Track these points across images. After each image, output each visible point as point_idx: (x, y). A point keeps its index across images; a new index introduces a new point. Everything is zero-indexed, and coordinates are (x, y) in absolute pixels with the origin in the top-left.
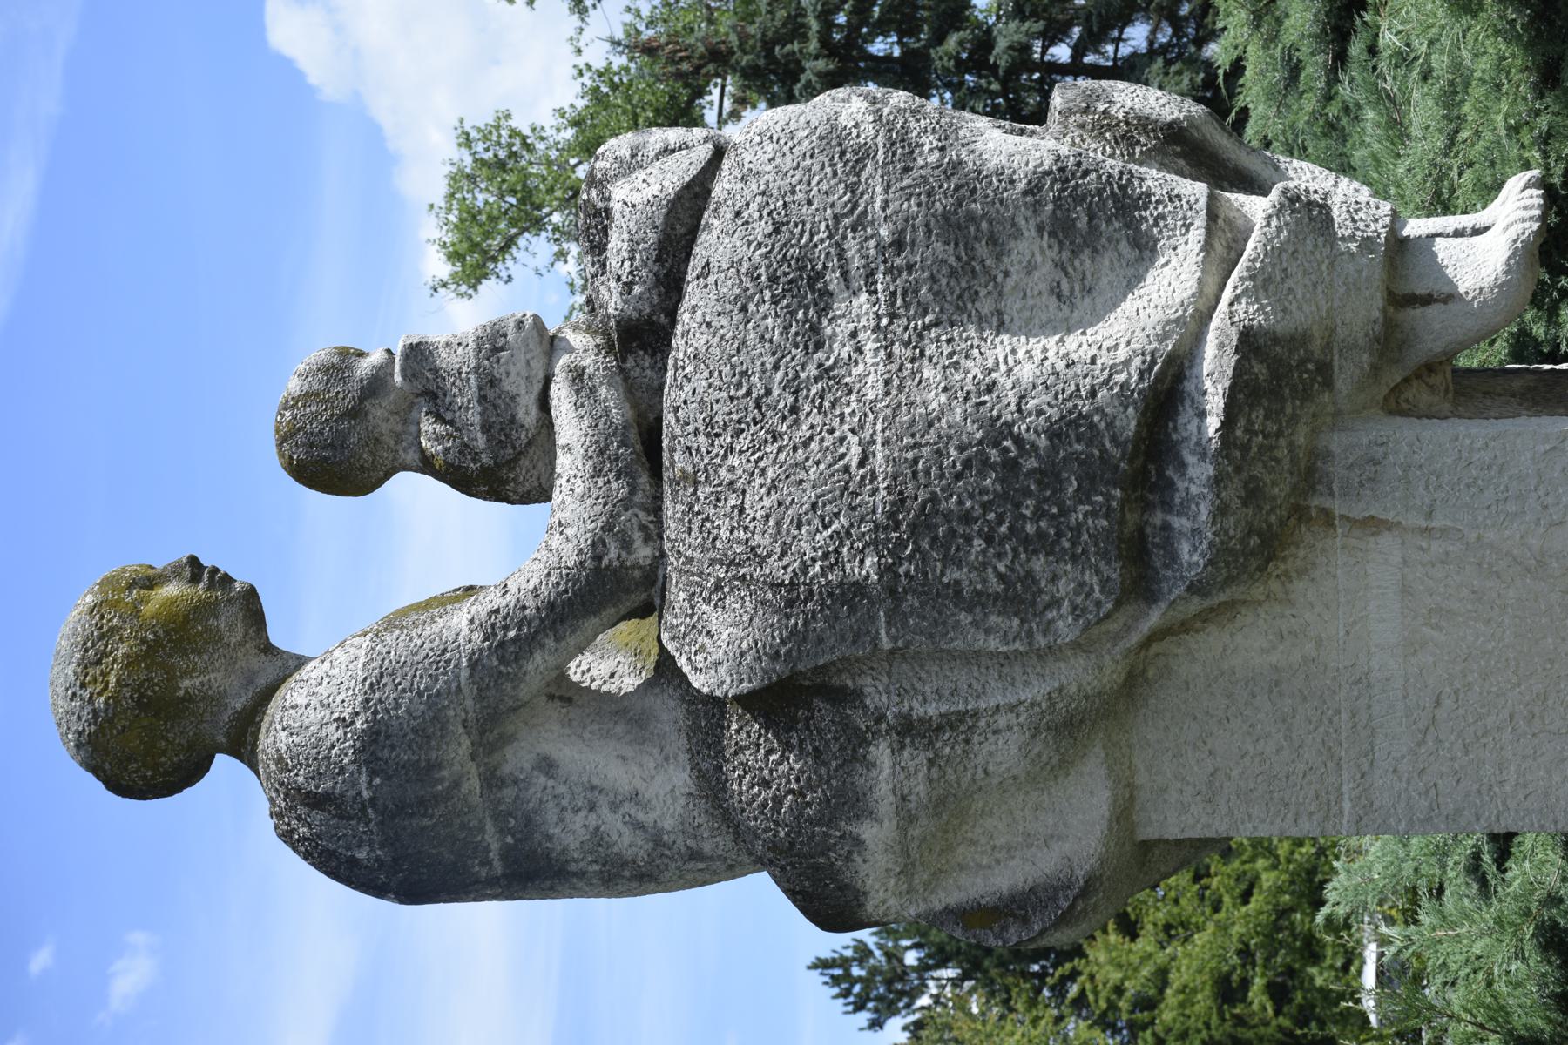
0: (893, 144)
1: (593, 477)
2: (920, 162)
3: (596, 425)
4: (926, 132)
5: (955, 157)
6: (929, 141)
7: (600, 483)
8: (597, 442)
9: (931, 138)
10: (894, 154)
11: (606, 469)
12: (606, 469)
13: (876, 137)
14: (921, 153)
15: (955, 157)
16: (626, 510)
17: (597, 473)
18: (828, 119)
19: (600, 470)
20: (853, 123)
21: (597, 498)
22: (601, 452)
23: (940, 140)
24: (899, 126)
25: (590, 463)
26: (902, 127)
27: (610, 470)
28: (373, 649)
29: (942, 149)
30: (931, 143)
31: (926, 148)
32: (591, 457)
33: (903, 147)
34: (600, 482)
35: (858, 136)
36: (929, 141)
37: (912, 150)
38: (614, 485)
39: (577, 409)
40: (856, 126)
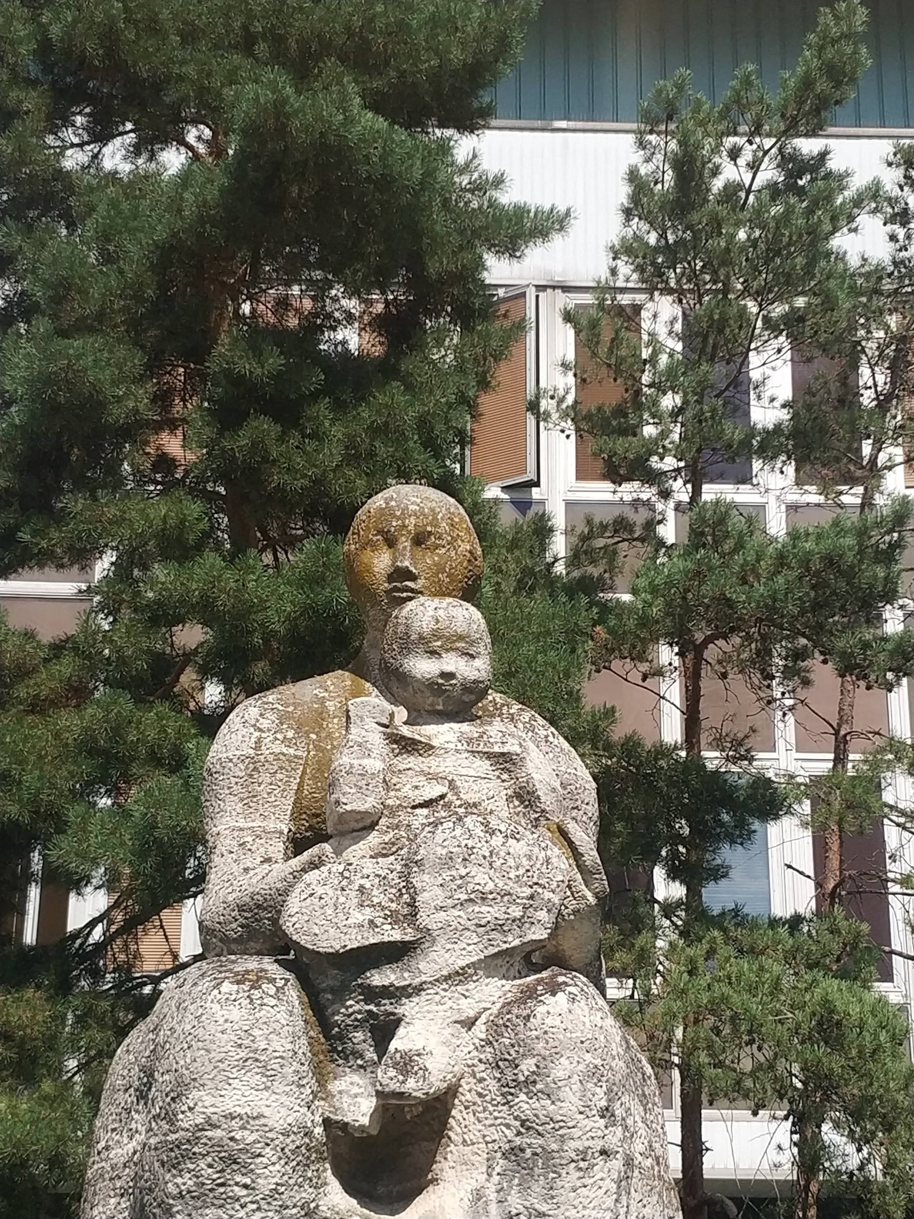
0: (178, 1147)
1: (238, 906)
2: (168, 1176)
3: (280, 895)
4: (198, 1177)
5: (175, 1209)
6: (187, 1181)
7: (233, 914)
8: (265, 899)
9: (190, 1183)
10: (172, 1150)
11: (246, 914)
12: (246, 914)
13: (182, 1129)
14: (174, 1176)
15: (175, 1209)
16: (221, 940)
17: (241, 908)
18: (195, 1080)
19: (243, 910)
20: (192, 1105)
21: (223, 915)
22: (259, 906)
23: (189, 1192)
24: (196, 1149)
25: (248, 900)
26: (194, 1154)
27: (246, 918)
28: (231, 760)
29: (182, 1197)
30: (184, 1184)
31: (179, 1180)
32: (253, 899)
33: (176, 1158)
34: (236, 912)
35: (183, 1112)
36: (187, 1181)
37: (174, 1166)
38: (234, 925)
39: (291, 873)
40: (190, 1109)
